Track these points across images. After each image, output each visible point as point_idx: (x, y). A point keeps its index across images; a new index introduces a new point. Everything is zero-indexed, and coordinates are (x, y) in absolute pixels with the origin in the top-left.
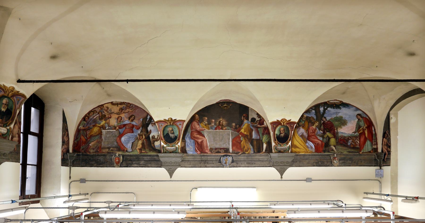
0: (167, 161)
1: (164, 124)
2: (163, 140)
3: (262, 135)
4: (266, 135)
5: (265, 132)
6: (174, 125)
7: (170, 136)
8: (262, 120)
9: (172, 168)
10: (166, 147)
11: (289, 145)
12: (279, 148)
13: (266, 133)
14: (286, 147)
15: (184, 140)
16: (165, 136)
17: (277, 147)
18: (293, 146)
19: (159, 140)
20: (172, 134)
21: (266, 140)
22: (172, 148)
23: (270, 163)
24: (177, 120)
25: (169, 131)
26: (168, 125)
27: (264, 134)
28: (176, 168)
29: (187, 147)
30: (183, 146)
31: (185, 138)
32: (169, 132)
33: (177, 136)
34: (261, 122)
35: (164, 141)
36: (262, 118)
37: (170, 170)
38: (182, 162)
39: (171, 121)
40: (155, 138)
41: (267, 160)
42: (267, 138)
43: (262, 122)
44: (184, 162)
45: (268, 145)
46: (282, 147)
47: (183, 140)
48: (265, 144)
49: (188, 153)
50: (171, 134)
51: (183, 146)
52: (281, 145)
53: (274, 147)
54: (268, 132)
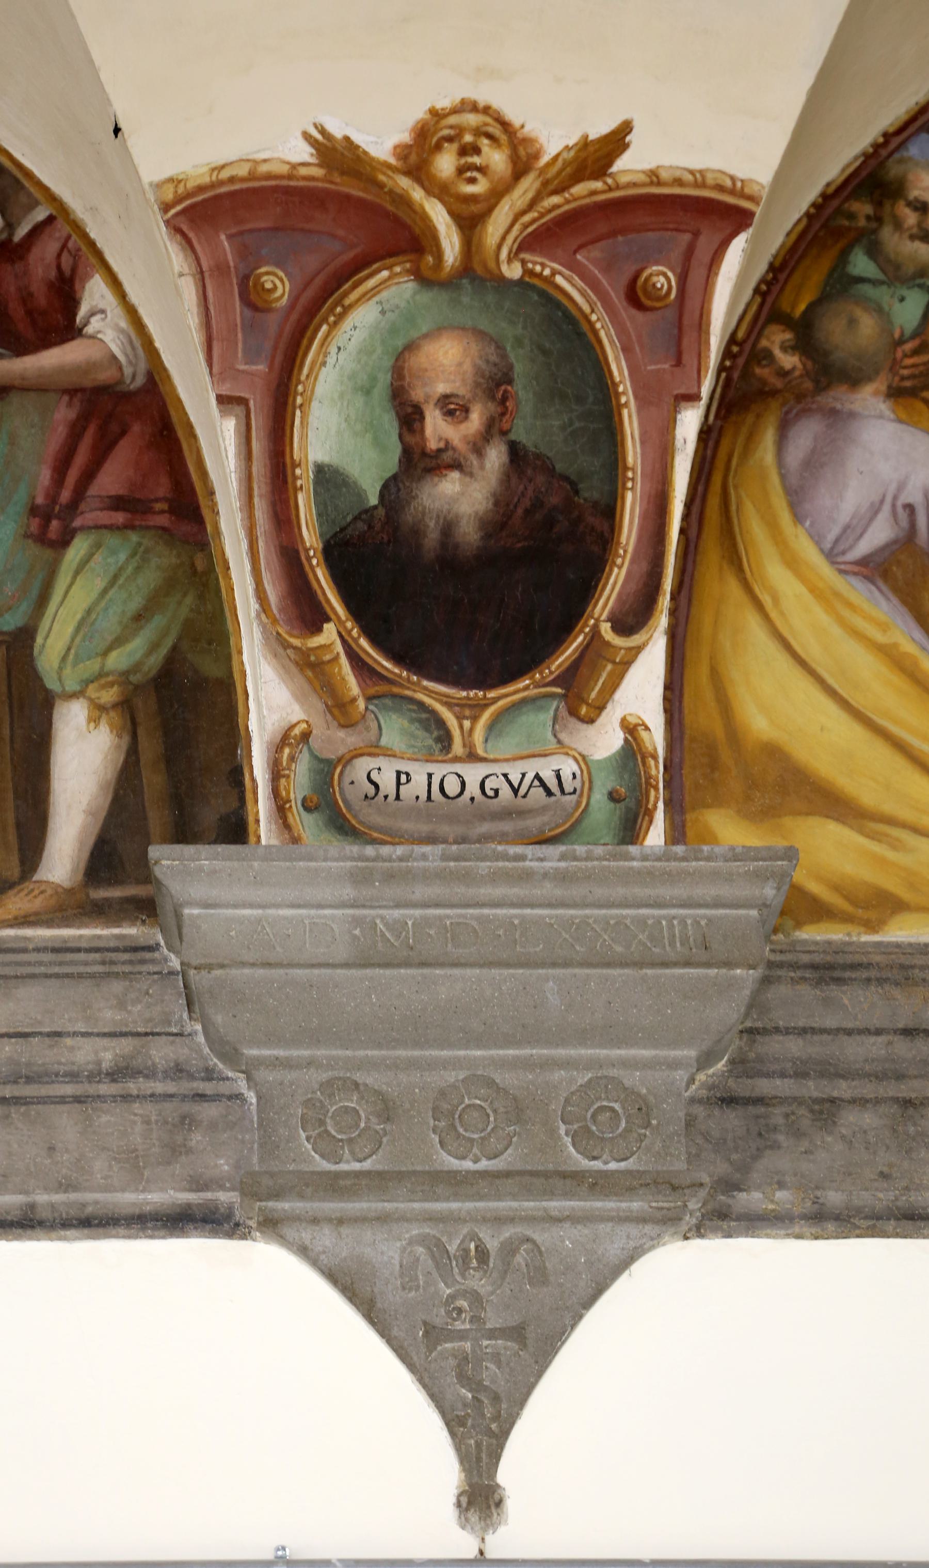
3: (41, 539)
4: (112, 540)
5: (89, 475)
8: (47, 249)
11: (631, 729)
12: (387, 781)
13: (118, 503)
14: (568, 767)
17: (347, 760)
18: (713, 763)
21: (118, 642)
23: (197, 1138)
27: (74, 505)
34: (26, 298)
36: (40, 214)
41: (117, 1074)
42: (136, 603)
43: (41, 299)
45: (150, 748)
46: (473, 774)
48: (98, 711)
52: (441, 723)
53: (277, 774)
54: (162, 488)
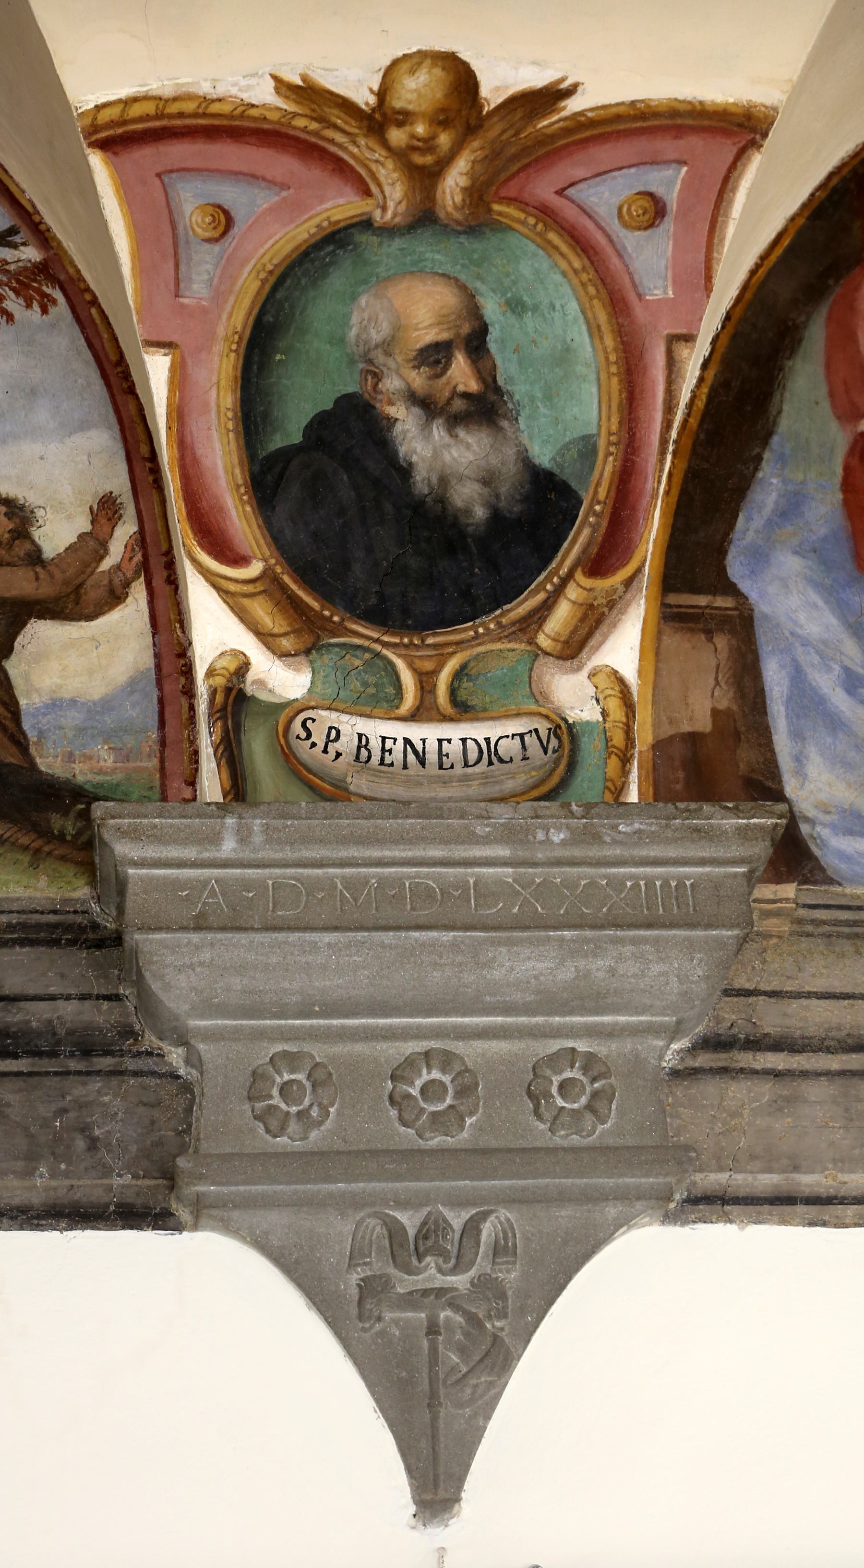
0: (318, 1052)
1: (271, 183)
2: (240, 560)
6: (500, 227)
7: (405, 472)
9: (457, 1219)
10: (297, 707)
15: (723, 602)
16: (286, 454)
19: (138, 594)
20: (454, 421)
22: (455, 732)
24: (574, 105)
25: (388, 346)
26: (366, 224)
28: (565, 1214)
29: (797, 735)
30: (703, 723)
31: (722, 570)
32: (392, 384)
33: (568, 475)
35: (255, 569)
37: (404, 1283)
38: (710, 1088)
39: (444, 140)
40: (35, 558)
44: (766, 1089)
47: (702, 600)
49: (829, 861)
50: (438, 432)
51: (703, 723)
